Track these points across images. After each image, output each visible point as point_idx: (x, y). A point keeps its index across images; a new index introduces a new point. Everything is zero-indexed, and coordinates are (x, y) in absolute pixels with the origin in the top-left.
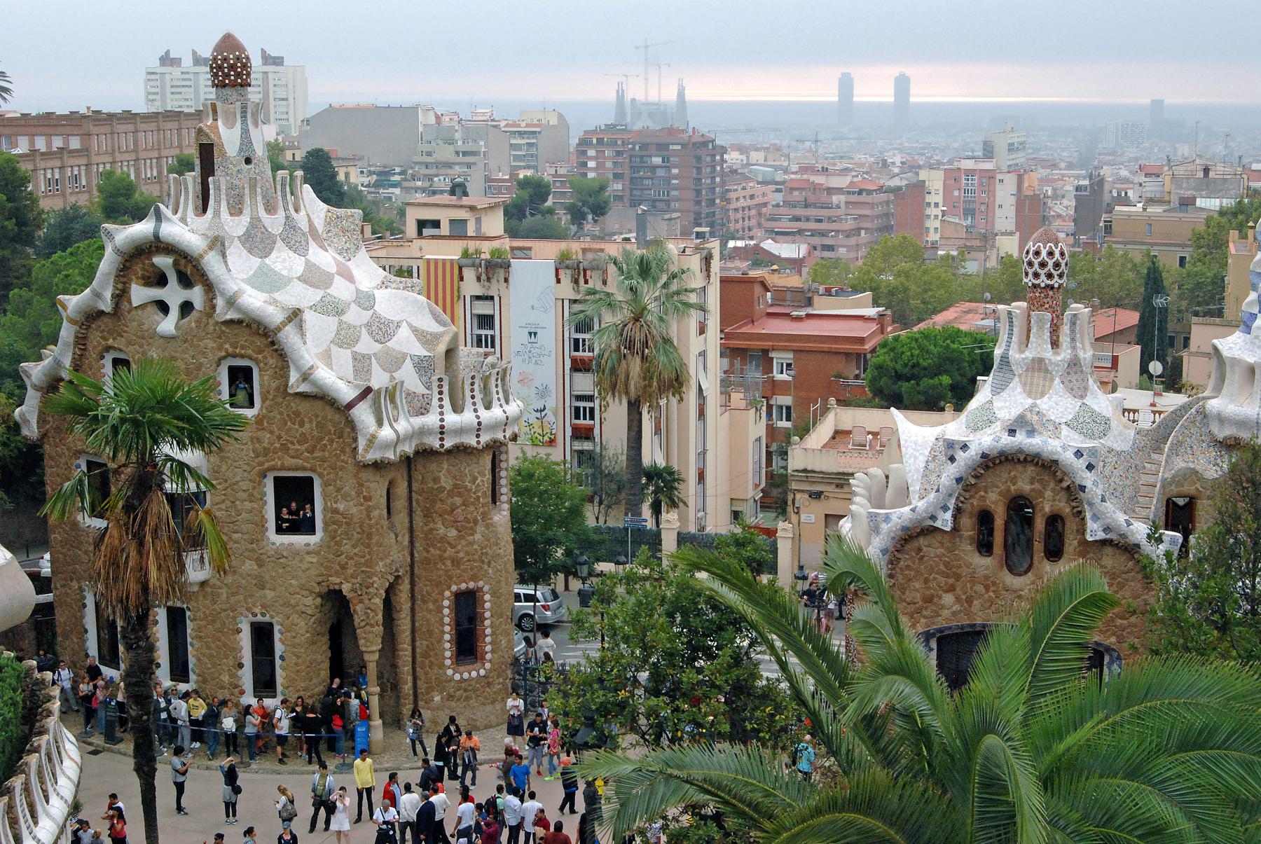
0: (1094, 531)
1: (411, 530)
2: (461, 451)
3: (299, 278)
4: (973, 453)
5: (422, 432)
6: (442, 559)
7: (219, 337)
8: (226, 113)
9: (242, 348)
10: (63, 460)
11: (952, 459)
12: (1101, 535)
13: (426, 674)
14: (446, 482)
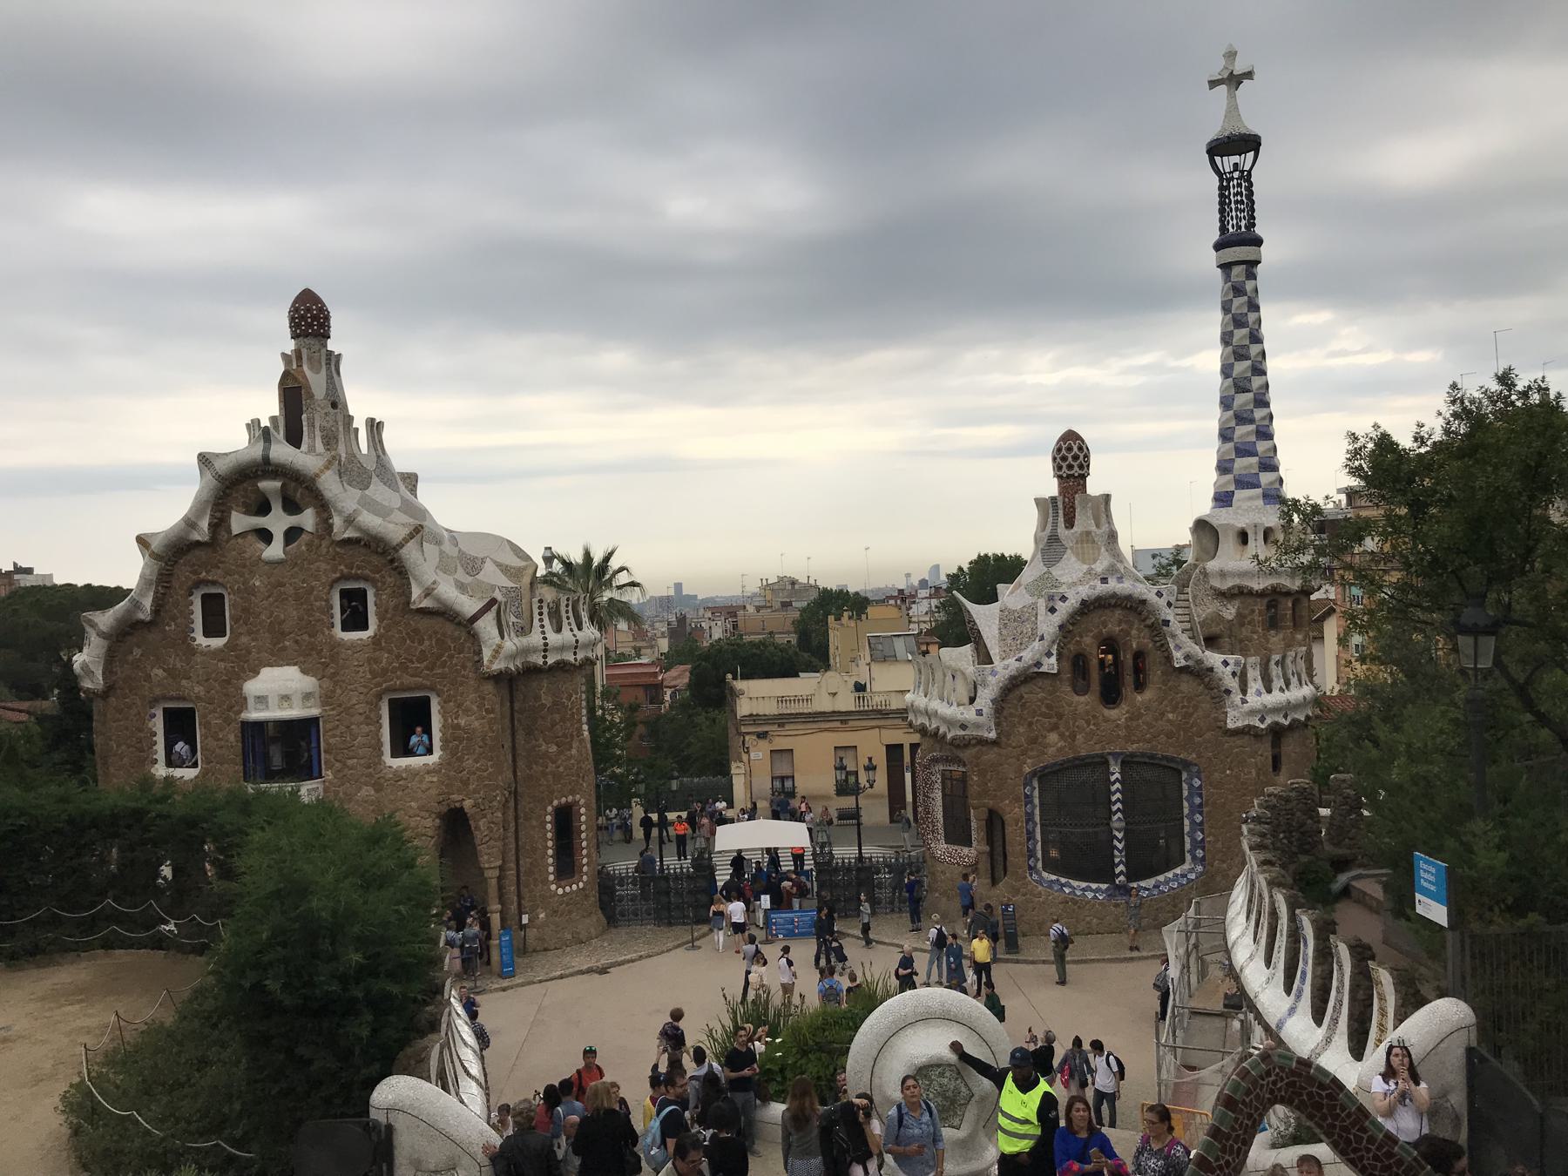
0: (1179, 660)
1: (514, 748)
2: (562, 666)
5: (526, 651)
6: (544, 774)
8: (310, 359)
10: (134, 711)
11: (1052, 610)
12: (1183, 663)
14: (547, 700)
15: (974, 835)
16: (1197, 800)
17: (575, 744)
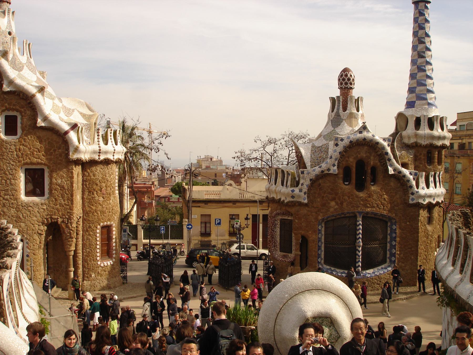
0: (391, 171)
1: (83, 198)
2: (107, 162)
3: (35, 82)
4: (346, 141)
7: (3, 100)
9: (14, 105)
11: (337, 145)
13: (88, 264)
15: (293, 248)
16: (394, 235)
17: (112, 198)
